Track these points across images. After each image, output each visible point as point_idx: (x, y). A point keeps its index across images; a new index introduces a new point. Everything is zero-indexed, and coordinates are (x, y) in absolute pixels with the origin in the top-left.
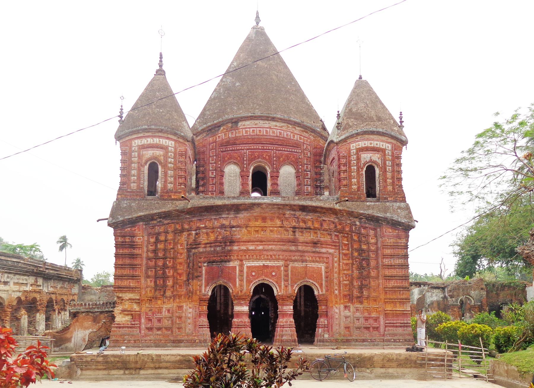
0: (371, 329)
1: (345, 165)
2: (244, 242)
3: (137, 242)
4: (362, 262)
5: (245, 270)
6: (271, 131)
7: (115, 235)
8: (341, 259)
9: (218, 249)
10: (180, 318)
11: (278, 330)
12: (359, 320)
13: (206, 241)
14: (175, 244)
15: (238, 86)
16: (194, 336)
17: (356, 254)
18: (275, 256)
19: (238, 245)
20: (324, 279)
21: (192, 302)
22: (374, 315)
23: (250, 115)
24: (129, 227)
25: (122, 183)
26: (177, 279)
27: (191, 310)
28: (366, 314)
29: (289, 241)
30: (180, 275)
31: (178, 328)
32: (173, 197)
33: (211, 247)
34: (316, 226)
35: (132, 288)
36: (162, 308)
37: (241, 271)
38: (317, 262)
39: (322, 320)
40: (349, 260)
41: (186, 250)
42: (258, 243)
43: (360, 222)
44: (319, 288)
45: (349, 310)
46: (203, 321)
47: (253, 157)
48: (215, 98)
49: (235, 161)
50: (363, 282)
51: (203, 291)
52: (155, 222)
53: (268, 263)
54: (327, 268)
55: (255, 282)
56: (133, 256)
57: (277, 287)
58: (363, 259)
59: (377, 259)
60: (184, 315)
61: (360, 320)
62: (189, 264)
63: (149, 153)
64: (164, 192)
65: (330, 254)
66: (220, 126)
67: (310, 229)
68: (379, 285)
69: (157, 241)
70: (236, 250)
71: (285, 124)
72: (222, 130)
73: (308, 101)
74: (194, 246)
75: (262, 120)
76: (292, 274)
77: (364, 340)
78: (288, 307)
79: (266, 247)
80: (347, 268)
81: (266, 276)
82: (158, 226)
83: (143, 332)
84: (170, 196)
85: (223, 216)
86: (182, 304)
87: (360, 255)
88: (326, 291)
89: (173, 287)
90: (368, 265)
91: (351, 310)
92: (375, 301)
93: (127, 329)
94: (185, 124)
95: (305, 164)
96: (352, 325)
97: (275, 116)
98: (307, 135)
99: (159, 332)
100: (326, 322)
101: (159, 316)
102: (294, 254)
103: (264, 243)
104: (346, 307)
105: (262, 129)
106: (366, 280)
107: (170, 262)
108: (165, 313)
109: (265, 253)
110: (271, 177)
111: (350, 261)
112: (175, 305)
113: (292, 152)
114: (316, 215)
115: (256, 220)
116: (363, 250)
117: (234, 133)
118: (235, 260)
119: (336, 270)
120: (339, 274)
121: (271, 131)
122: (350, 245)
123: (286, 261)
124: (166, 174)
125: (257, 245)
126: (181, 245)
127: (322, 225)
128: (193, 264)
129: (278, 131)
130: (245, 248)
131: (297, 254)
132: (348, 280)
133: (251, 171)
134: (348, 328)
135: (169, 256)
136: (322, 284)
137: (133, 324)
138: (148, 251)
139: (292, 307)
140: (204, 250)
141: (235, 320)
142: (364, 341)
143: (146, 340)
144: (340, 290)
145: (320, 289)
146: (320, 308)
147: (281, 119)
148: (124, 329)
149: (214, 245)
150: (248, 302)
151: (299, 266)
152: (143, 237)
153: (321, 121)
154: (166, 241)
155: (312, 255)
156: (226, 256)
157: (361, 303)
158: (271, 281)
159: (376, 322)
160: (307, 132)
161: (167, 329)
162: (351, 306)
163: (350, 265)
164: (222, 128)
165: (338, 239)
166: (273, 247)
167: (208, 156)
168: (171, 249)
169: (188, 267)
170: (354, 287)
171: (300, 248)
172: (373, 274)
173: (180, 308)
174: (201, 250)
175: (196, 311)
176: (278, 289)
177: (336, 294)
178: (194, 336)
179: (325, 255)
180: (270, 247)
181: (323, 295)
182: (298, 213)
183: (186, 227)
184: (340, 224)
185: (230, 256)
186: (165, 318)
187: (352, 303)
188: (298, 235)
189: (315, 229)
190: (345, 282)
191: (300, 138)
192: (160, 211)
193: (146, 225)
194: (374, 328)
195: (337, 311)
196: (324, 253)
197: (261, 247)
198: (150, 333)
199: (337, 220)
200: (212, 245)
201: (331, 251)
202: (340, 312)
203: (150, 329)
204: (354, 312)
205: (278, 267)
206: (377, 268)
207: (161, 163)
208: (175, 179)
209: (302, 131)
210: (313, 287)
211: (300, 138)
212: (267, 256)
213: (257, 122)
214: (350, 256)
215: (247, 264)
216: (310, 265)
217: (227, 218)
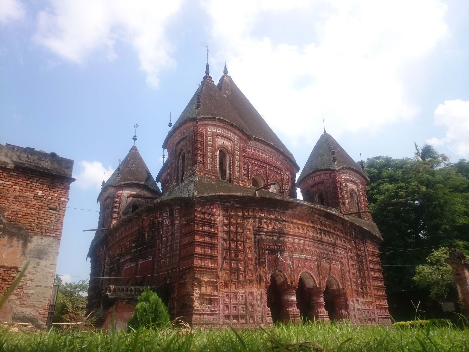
1: (340, 188)
2: (292, 235)
3: (214, 221)
10: (252, 305)
30: (250, 259)
33: (270, 235)
35: (211, 269)
43: (355, 233)
45: (358, 303)
47: (254, 169)
52: (229, 204)
56: (212, 235)
68: (370, 284)
69: (230, 224)
71: (274, 151)
75: (261, 143)
84: (239, 183)
85: (277, 210)
86: (253, 290)
97: (269, 142)
98: (286, 163)
99: (235, 321)
101: (234, 301)
112: (248, 290)
126: (249, 229)
128: (259, 250)
137: (211, 311)
138: (223, 231)
147: (273, 146)
148: (205, 316)
152: (219, 216)
156: (281, 246)
157: (363, 297)
160: (286, 161)
168: (241, 232)
171: (325, 247)
173: (252, 293)
182: (322, 218)
185: (284, 246)
188: (323, 236)
198: (228, 321)
207: (229, 152)
208: (241, 169)
209: (284, 159)
213: (257, 143)
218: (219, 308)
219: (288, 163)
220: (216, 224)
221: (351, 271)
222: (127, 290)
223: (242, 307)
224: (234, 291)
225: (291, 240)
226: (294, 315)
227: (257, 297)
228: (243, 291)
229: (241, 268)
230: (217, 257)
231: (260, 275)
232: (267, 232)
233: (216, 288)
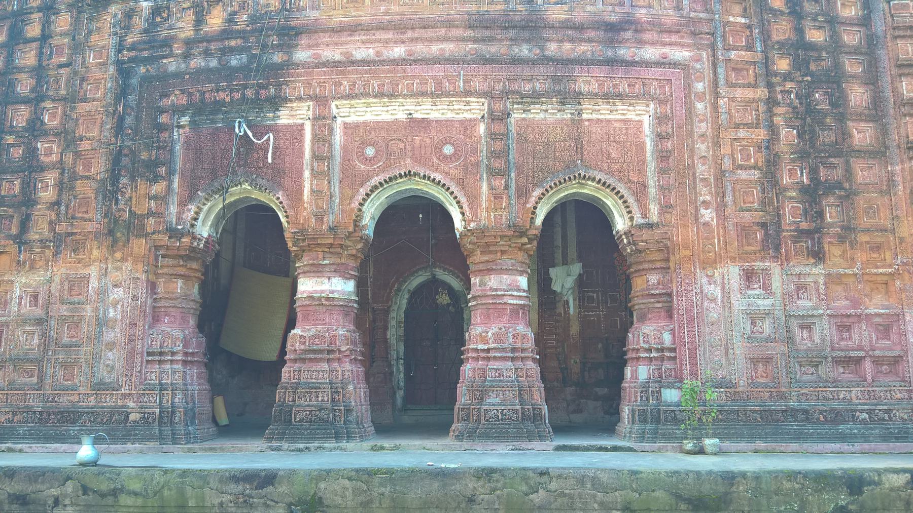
0: (868, 365)
4: (809, 95)
5: (338, 138)
8: (722, 81)
9: (234, 61)
10: (75, 324)
11: (467, 369)
12: (809, 327)
13: (189, 33)
14: (78, 47)
16: (124, 396)
17: (783, 65)
19: (309, 47)
20: (651, 166)
21: (124, 259)
22: (875, 305)
26: (74, 177)
28: (841, 305)
29: (508, 25)
31: (65, 365)
33: (207, 54)
37: (322, 139)
38: (621, 97)
39: (648, 329)
40: (755, 86)
41: (112, 70)
42: (390, 35)
44: (631, 200)
45: (767, 288)
46: (166, 335)
50: (823, 172)
53: (427, 110)
54: (661, 119)
55: (376, 180)
57: (463, 200)
58: (816, 82)
59: (872, 79)
61: (817, 331)
62: (121, 119)
65: (675, 65)
68: (891, 182)
70: (304, 65)
74: (146, 54)
77: (838, 413)
78: (507, 279)
80: (750, 118)
81: (417, 160)
86: (86, 271)
87: (800, 64)
88: (666, 208)
89: (58, 203)
90: (838, 101)
91: (776, 283)
92: (877, 248)
96: (782, 348)
100: (667, 338)
102: (527, 71)
103: (410, 34)
104: (749, 276)
106: (833, 167)
107: (53, 116)
109: (411, 70)
111: (762, 92)
116: (812, 47)
118: (300, 99)
119: (702, 127)
120: (717, 143)
122: (756, 31)
128: (138, 119)
130: (337, 57)
131: (540, 70)
132: (755, 167)
134: (767, 360)
135: (50, 93)
136: (645, 186)
139: (523, 281)
140: (183, 65)
142: (836, 417)
144: (721, 208)
145: (635, 208)
146: (638, 284)
149: (219, 45)
150: (352, 263)
151: (550, 119)
154: (45, 37)
155: (600, 72)
156: (266, 87)
157: (818, 255)
158: (438, 177)
159: (887, 336)
162: (776, 270)
163: (762, 107)
165: (706, 11)
166: (449, 48)
168: (61, 66)
169: (119, 129)
170: (781, 191)
171: (552, 48)
172: (862, 134)
174: (172, 65)
176: (466, 208)
177: (706, 224)
179: (654, 72)
180: (436, 48)
181: (650, 226)
185: (278, 86)
187: (776, 257)
190: (743, 175)
194: (877, 361)
195: (715, 291)
196: (647, 64)
197: (398, 51)
200: (213, 46)
201: (680, 54)
202: (726, 294)
204: (787, 295)
205: (467, 126)
206: (876, 112)
212: (424, 82)
214: (761, 71)
215: (350, 113)
216: (592, 112)
221: (727, 135)
225: (332, 54)
226: (306, 351)
227: (102, 292)
228: (36, 279)
231: (130, 211)
232: (188, 43)
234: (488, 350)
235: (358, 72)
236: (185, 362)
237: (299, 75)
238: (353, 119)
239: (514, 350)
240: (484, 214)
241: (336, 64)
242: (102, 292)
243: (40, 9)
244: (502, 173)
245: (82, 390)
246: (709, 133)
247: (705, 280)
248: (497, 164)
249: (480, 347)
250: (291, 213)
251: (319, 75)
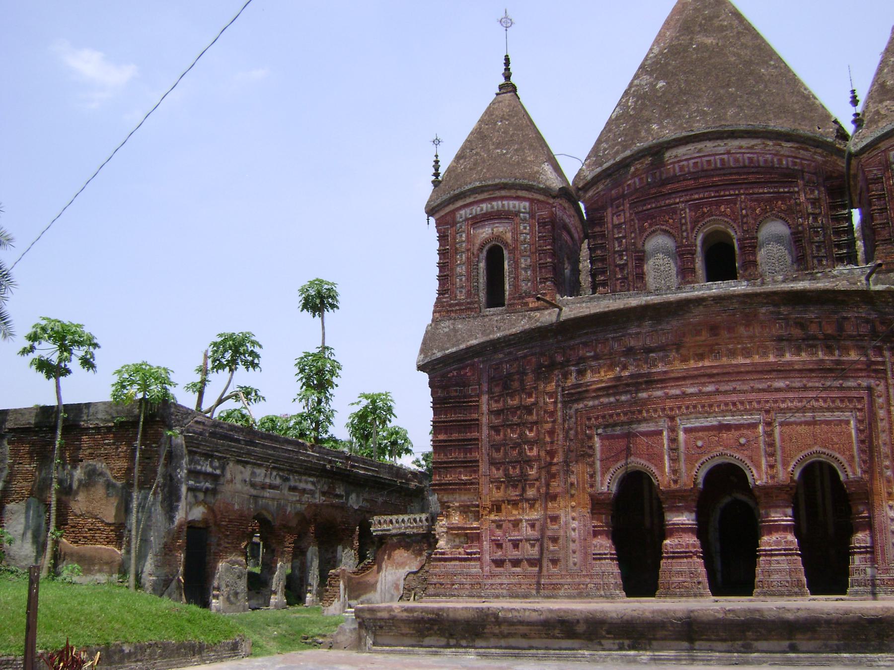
2: (677, 379)
3: (471, 396)
6: (731, 159)
7: (431, 385)
9: (623, 398)
15: (661, 88)
16: (584, 576)
18: (742, 403)
19: (662, 388)
23: (684, 134)
24: (455, 370)
25: (442, 292)
27: (576, 522)
32: (531, 306)
33: (608, 395)
34: (830, 332)
35: (465, 484)
36: (521, 520)
39: (860, 535)
44: (846, 466)
48: (618, 118)
49: (664, 227)
51: (598, 484)
52: (501, 356)
53: (728, 419)
55: (703, 459)
60: (562, 533)
62: (567, 432)
63: (485, 232)
64: (514, 298)
66: (628, 166)
67: (815, 338)
72: (634, 173)
73: (806, 89)
75: (710, 140)
76: (782, 440)
79: (724, 387)
81: (726, 447)
82: (507, 362)
83: (487, 569)
84: (527, 304)
85: (629, 331)
93: (457, 563)
94: (547, 167)
95: (809, 214)
99: (518, 569)
100: (868, 539)
101: (515, 535)
105: (712, 158)
108: (527, 531)
109: (720, 398)
110: (740, 249)
113: (779, 193)
114: (826, 307)
115: (698, 333)
117: (658, 174)
121: (731, 159)
123: (767, 412)
124: (516, 264)
125: (703, 384)
127: (841, 328)
128: (577, 432)
129: (746, 156)
133: (699, 242)
136: (853, 457)
137: (468, 554)
141: (667, 541)
143: (492, 584)
145: (848, 469)
148: (453, 563)
150: (694, 504)
153: (836, 122)
160: (806, 150)
161: (532, 562)
164: (632, 169)
167: (610, 226)
173: (555, 519)
175: (585, 526)
178: (584, 576)
182: (784, 310)
183: (560, 359)
184: (882, 323)
186: (527, 540)
189: (827, 337)
191: (795, 164)
192: (507, 332)
193: (483, 362)
197: (710, 388)
199: (873, 316)
203: (499, 563)
207: (507, 245)
208: (534, 271)
210: (835, 465)
211: (795, 164)
212: (726, 404)
213: (699, 146)
217: (638, 334)
218: (481, 548)
219: (815, 153)
220: (474, 401)
222: (397, 522)
223: (533, 546)
224: (513, 518)
225: (676, 391)
227: (566, 523)
229: (533, 472)
230: (478, 461)
233: (478, 517)
234: (771, 550)
235: (689, 400)
236: (612, 559)
237: (658, 404)
238: (688, 425)
239: (785, 550)
240: (764, 477)
241: (676, 397)
242: (566, 523)
243: (518, 373)
244: (772, 455)
245: (563, 573)
246: (887, 426)
247: (888, 509)
248: (769, 450)
249: (767, 548)
250: (659, 478)
251: (669, 404)
